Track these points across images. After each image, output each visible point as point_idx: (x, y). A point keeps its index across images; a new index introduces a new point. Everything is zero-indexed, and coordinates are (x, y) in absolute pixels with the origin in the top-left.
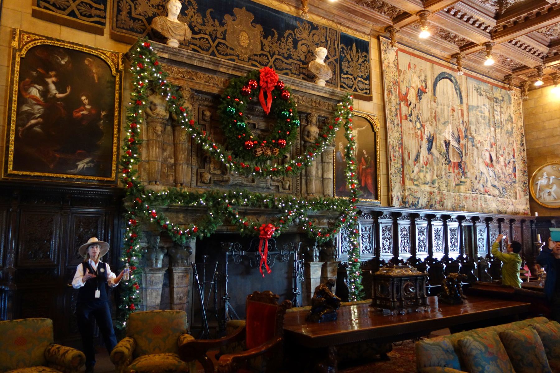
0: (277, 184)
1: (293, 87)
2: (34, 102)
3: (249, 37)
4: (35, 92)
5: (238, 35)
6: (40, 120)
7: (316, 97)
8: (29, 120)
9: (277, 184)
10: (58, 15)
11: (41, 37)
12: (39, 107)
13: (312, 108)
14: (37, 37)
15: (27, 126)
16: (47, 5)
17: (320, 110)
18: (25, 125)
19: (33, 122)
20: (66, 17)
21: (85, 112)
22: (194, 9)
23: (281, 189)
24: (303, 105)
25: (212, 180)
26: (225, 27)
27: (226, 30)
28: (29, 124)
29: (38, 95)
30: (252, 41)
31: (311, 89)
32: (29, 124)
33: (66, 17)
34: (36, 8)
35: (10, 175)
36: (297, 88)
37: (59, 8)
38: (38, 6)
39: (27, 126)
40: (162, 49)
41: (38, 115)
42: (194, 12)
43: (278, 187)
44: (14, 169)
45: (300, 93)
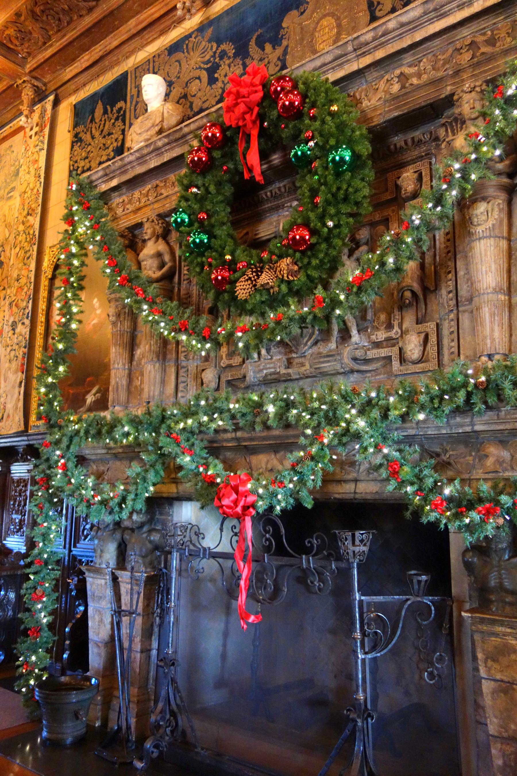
0: (383, 352)
1: (367, 60)
3: (338, 19)
5: (312, 34)
7: (474, 27)
9: (383, 352)
13: (457, 73)
17: (491, 58)
21: (95, 321)
22: (229, 58)
23: (396, 364)
24: (419, 87)
25: (223, 380)
26: (285, 43)
27: (287, 46)
30: (344, 22)
31: (431, 21)
36: (380, 54)
40: (106, 175)
42: (229, 66)
43: (388, 359)
45: (408, 58)
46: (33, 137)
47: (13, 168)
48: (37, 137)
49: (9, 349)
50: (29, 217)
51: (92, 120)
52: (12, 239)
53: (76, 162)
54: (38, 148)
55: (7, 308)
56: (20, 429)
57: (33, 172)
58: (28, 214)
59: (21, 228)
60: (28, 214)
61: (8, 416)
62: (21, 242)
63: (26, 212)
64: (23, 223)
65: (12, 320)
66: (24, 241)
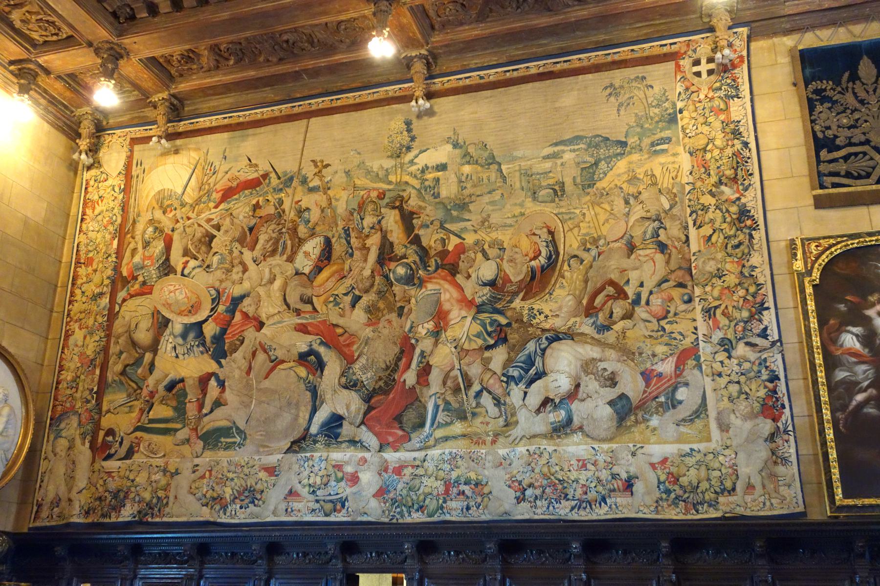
2: (854, 360)
4: (850, 340)
6: (872, 391)
8: (851, 400)
10: (859, 189)
11: (839, 239)
12: (864, 367)
14: (832, 241)
15: (851, 408)
16: (836, 180)
18: (847, 406)
19: (860, 397)
20: (874, 187)
28: (854, 403)
29: (858, 346)
32: (854, 403)
33: (874, 187)
34: (820, 192)
35: (842, 508)
37: (859, 177)
38: (822, 187)
39: (851, 408)
41: (866, 383)
44: (846, 495)
46: (704, 75)
47: (657, 111)
48: (713, 77)
49: (723, 381)
50: (723, 188)
51: (854, 77)
52: (683, 211)
53: (829, 128)
54: (722, 93)
55: (699, 315)
56: (798, 510)
57: (717, 125)
58: (720, 182)
59: (708, 200)
60: (720, 182)
61: (750, 487)
62: (712, 221)
63: (714, 179)
64: (713, 195)
65: (718, 335)
66: (719, 220)
